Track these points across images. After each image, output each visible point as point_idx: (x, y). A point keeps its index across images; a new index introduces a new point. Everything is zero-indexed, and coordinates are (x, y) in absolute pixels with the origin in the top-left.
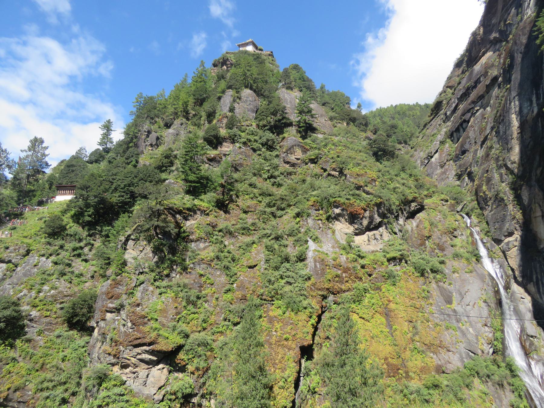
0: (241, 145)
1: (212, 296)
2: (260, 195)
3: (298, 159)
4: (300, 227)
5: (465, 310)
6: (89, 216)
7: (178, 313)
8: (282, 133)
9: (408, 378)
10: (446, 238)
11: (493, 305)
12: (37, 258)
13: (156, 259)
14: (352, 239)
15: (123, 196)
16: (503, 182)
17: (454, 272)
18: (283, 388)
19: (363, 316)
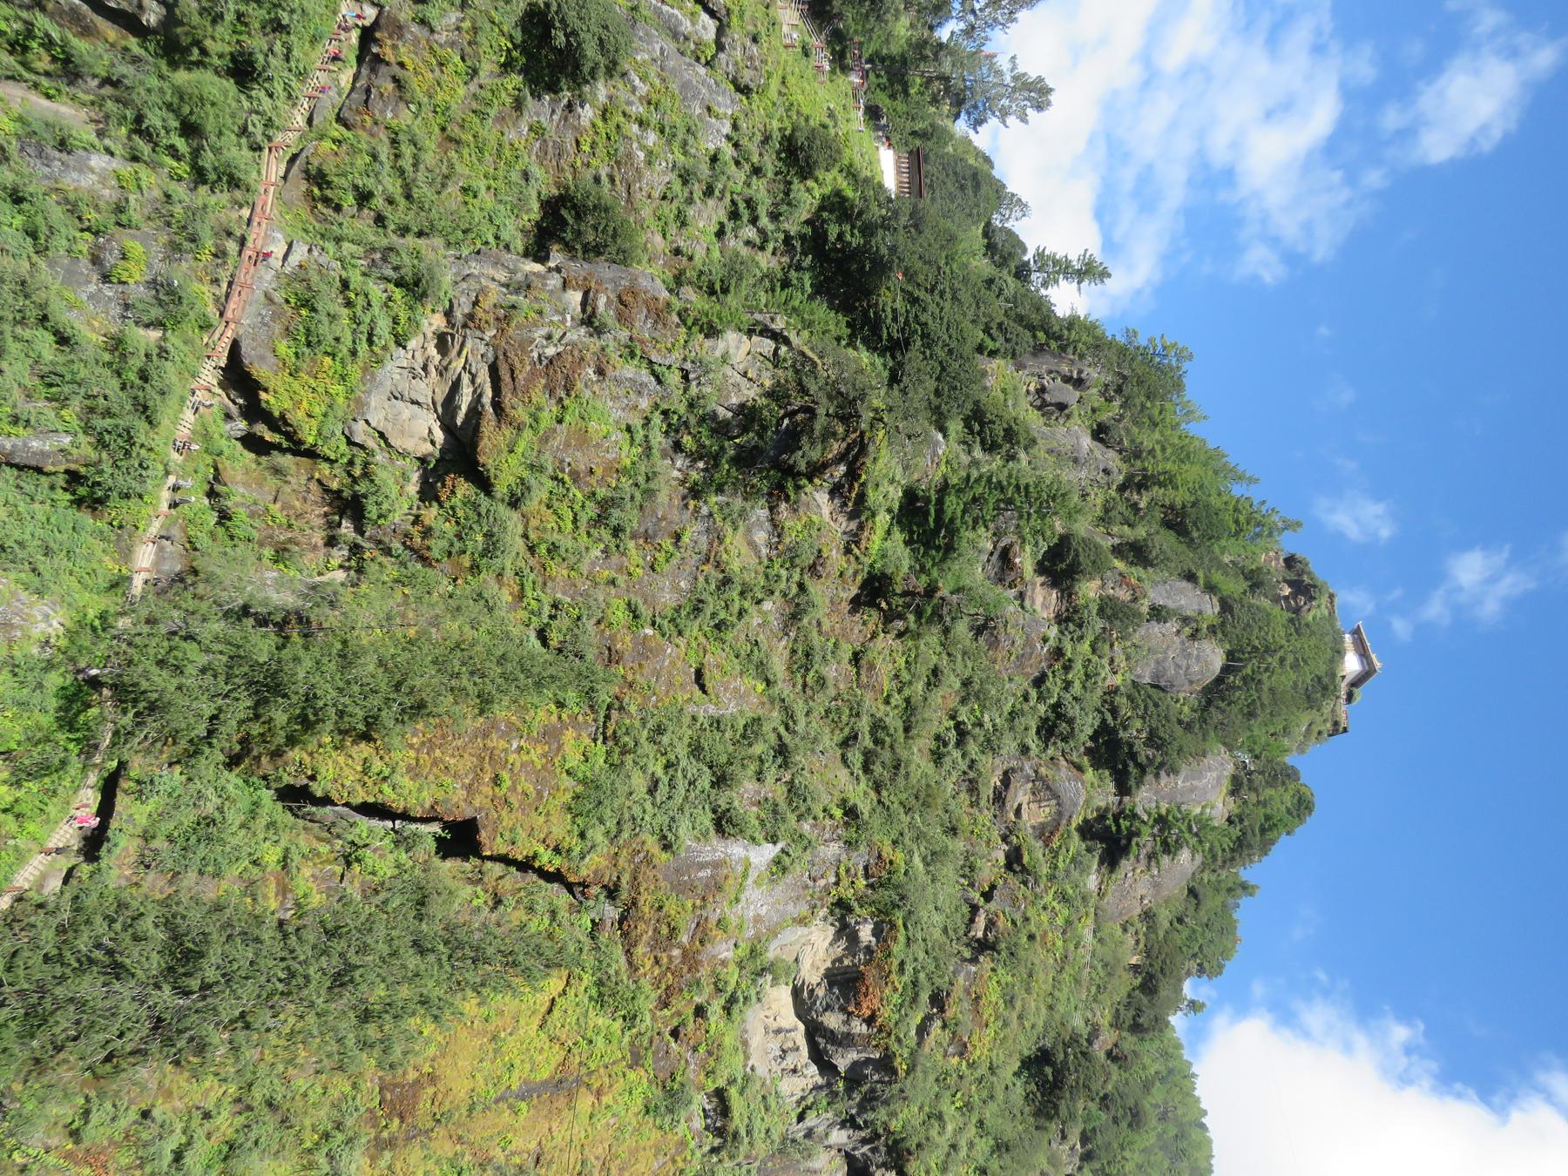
0: (1052, 643)
1: (620, 569)
2: (908, 700)
3: (1018, 812)
4: (815, 818)
6: (840, 236)
7: (575, 476)
8: (1096, 765)
12: (730, 112)
13: (723, 413)
14: (783, 980)
15: (895, 319)
18: (365, 772)
19: (556, 1012)
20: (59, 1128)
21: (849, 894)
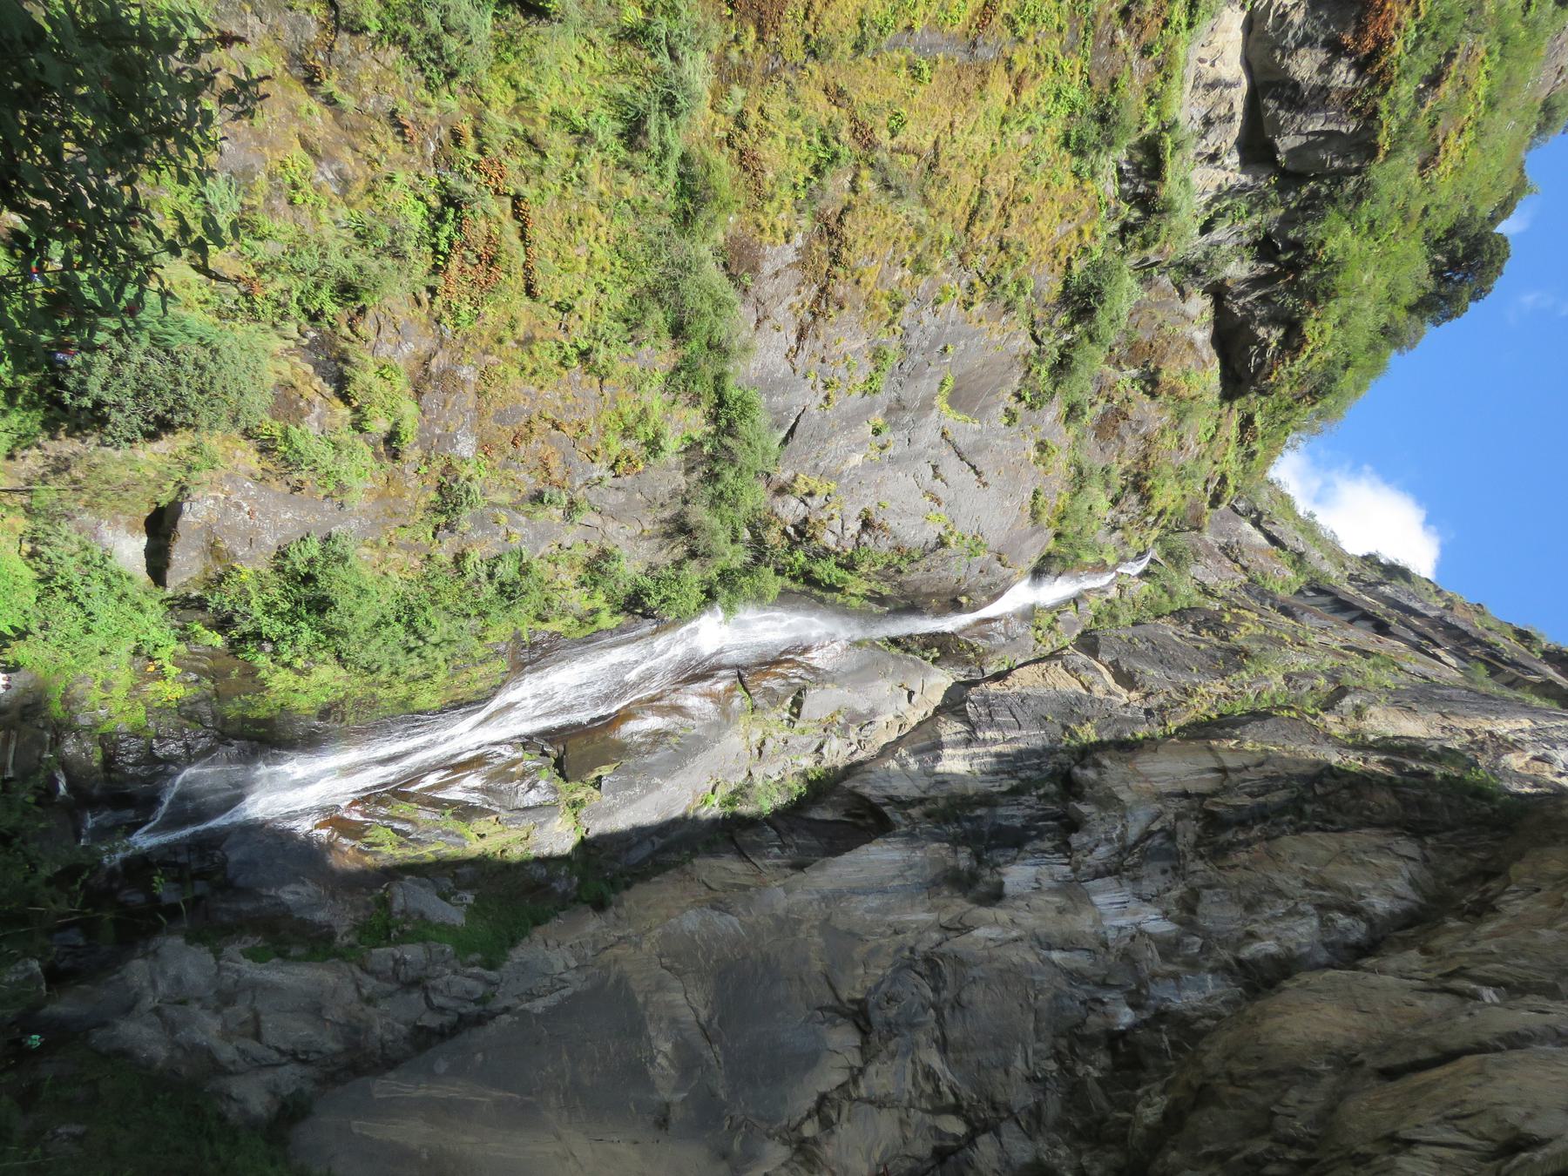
9: (719, 72)
10: (1122, 462)
11: (915, 576)
16: (1288, 678)
17: (1042, 447)
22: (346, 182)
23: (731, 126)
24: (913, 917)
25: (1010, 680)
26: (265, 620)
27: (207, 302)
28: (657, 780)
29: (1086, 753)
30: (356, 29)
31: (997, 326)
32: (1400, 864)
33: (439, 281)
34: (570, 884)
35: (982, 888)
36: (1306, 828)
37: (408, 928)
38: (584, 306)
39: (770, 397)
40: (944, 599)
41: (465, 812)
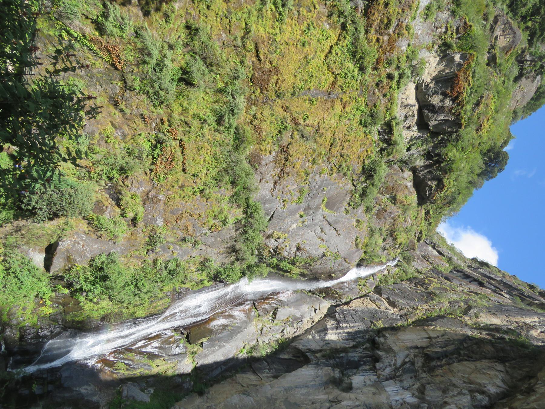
3: (496, 38)
5: (316, 225)
9: (248, 102)
10: (386, 227)
11: (316, 267)
16: (450, 303)
17: (358, 221)
19: (333, 51)
20: (89, 22)
21: (449, 40)
22: (125, 136)
23: (252, 118)
24: (319, 397)
25: (351, 305)
26: (84, 284)
27: (75, 174)
28: (223, 343)
29: (380, 332)
30: (132, 89)
31: (341, 181)
32: (497, 373)
33: (154, 167)
34: (190, 384)
35: (344, 385)
36: (462, 360)
37: (128, 403)
38: (202, 175)
39: (265, 205)
40: (326, 275)
41: (152, 356)
